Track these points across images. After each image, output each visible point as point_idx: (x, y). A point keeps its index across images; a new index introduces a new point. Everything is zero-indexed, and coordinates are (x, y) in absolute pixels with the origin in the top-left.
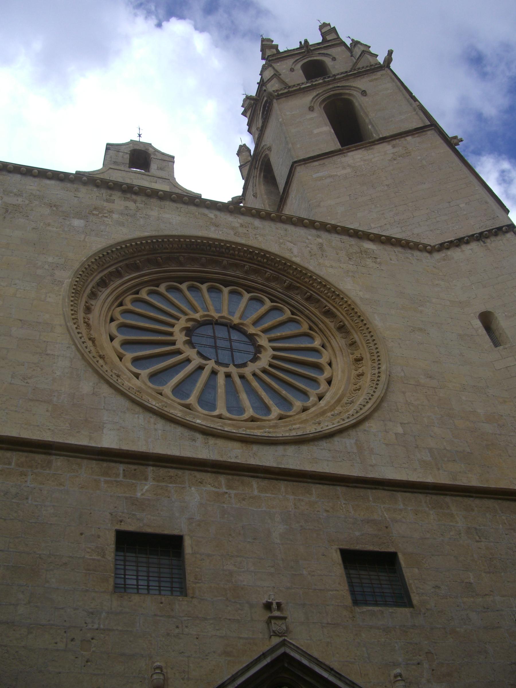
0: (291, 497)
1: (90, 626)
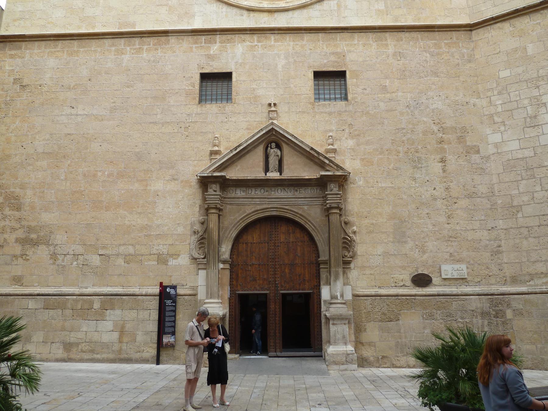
0: (292, 43)
1: (188, 121)
